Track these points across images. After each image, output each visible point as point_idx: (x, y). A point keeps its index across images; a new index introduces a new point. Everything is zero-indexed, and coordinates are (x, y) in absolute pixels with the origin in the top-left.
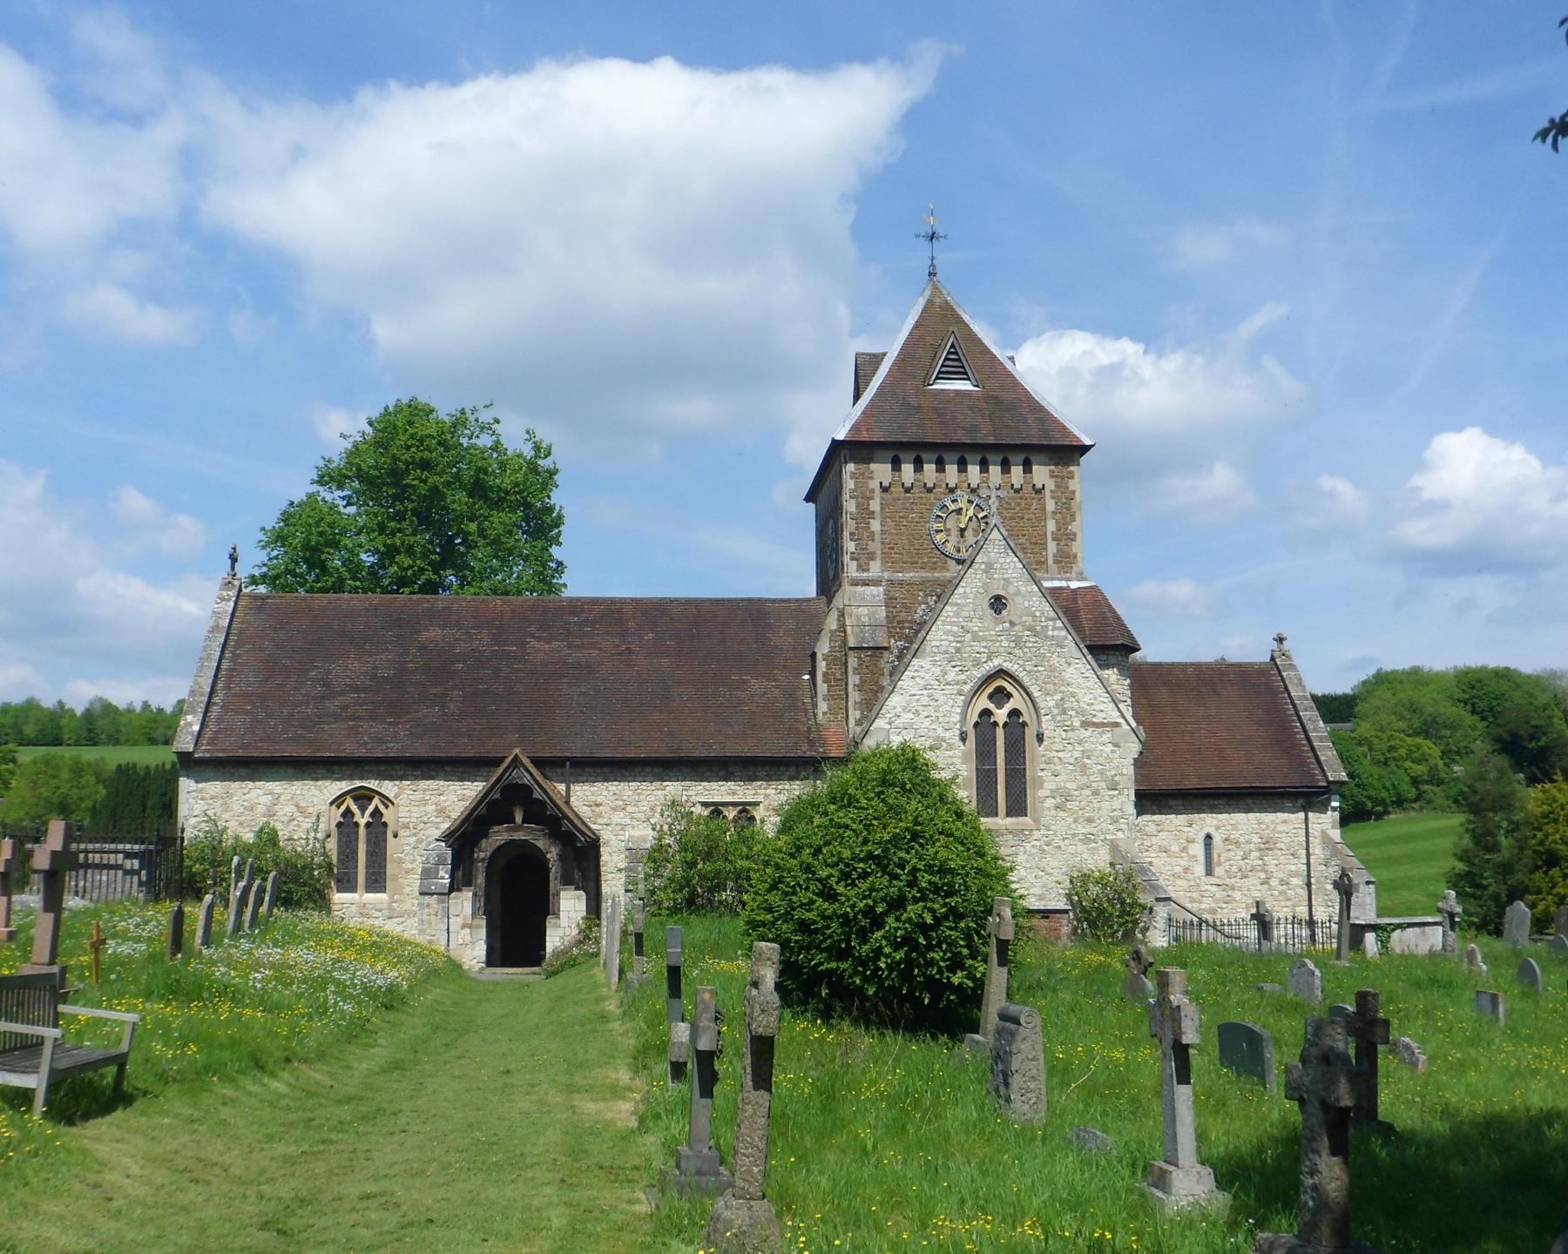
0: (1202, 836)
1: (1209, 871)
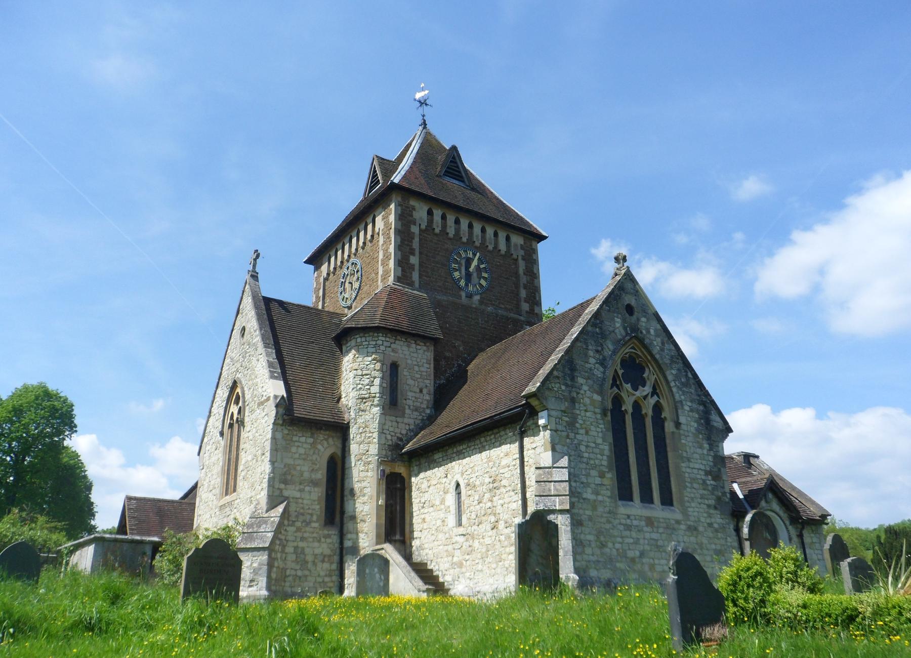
1: (460, 524)
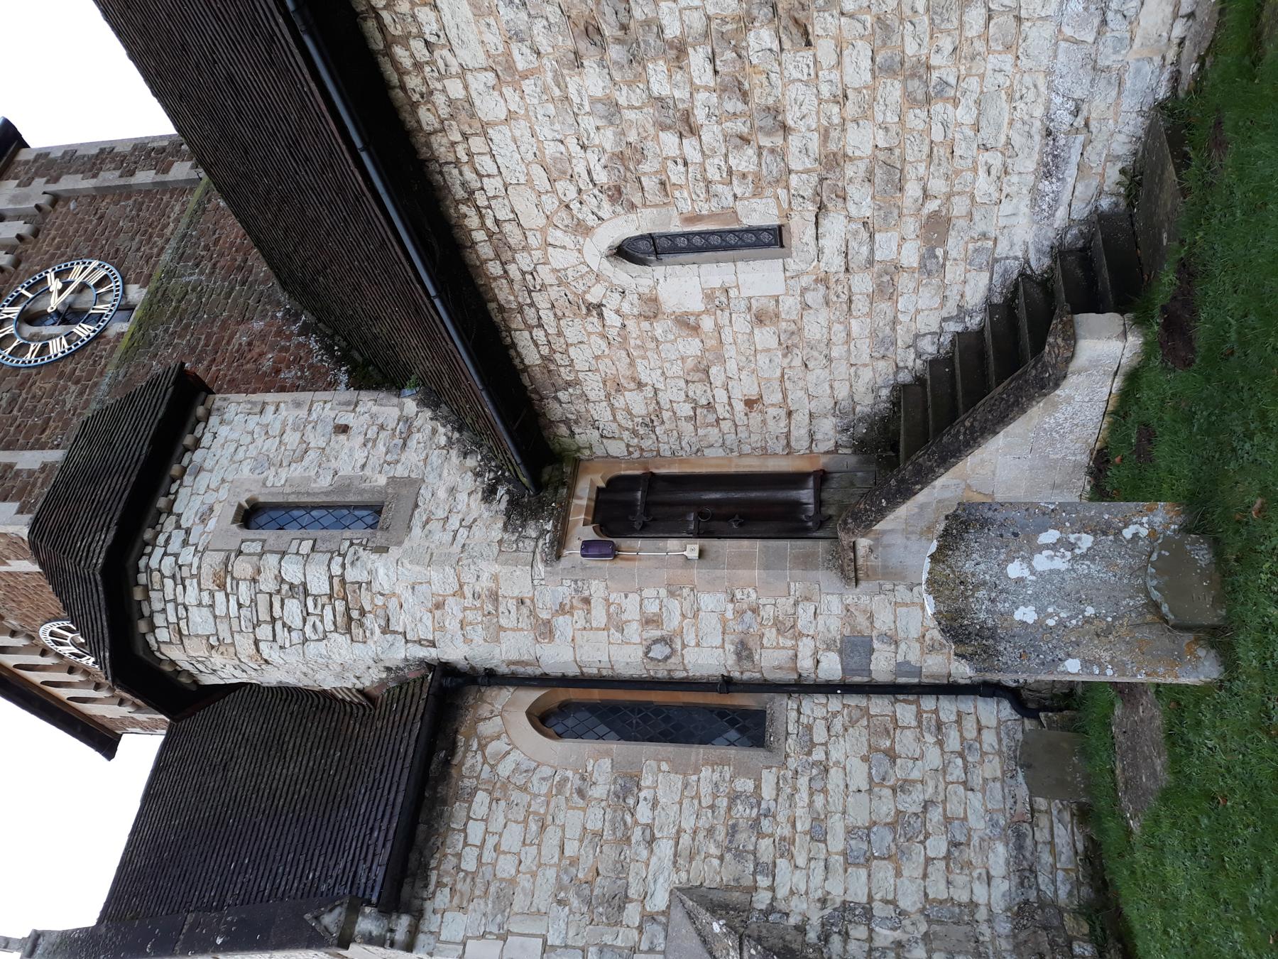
0: (625, 274)
1: (772, 239)
